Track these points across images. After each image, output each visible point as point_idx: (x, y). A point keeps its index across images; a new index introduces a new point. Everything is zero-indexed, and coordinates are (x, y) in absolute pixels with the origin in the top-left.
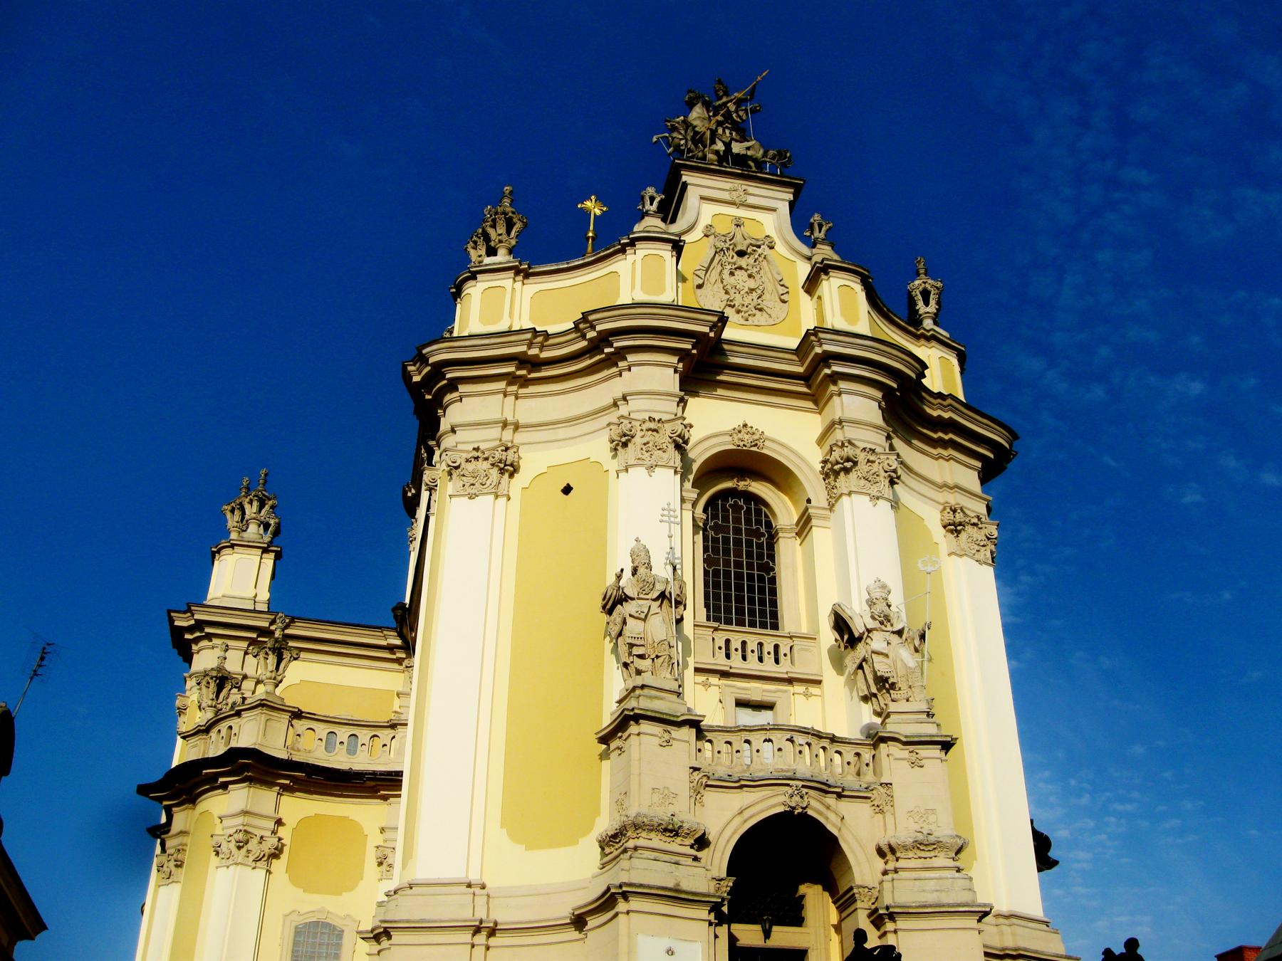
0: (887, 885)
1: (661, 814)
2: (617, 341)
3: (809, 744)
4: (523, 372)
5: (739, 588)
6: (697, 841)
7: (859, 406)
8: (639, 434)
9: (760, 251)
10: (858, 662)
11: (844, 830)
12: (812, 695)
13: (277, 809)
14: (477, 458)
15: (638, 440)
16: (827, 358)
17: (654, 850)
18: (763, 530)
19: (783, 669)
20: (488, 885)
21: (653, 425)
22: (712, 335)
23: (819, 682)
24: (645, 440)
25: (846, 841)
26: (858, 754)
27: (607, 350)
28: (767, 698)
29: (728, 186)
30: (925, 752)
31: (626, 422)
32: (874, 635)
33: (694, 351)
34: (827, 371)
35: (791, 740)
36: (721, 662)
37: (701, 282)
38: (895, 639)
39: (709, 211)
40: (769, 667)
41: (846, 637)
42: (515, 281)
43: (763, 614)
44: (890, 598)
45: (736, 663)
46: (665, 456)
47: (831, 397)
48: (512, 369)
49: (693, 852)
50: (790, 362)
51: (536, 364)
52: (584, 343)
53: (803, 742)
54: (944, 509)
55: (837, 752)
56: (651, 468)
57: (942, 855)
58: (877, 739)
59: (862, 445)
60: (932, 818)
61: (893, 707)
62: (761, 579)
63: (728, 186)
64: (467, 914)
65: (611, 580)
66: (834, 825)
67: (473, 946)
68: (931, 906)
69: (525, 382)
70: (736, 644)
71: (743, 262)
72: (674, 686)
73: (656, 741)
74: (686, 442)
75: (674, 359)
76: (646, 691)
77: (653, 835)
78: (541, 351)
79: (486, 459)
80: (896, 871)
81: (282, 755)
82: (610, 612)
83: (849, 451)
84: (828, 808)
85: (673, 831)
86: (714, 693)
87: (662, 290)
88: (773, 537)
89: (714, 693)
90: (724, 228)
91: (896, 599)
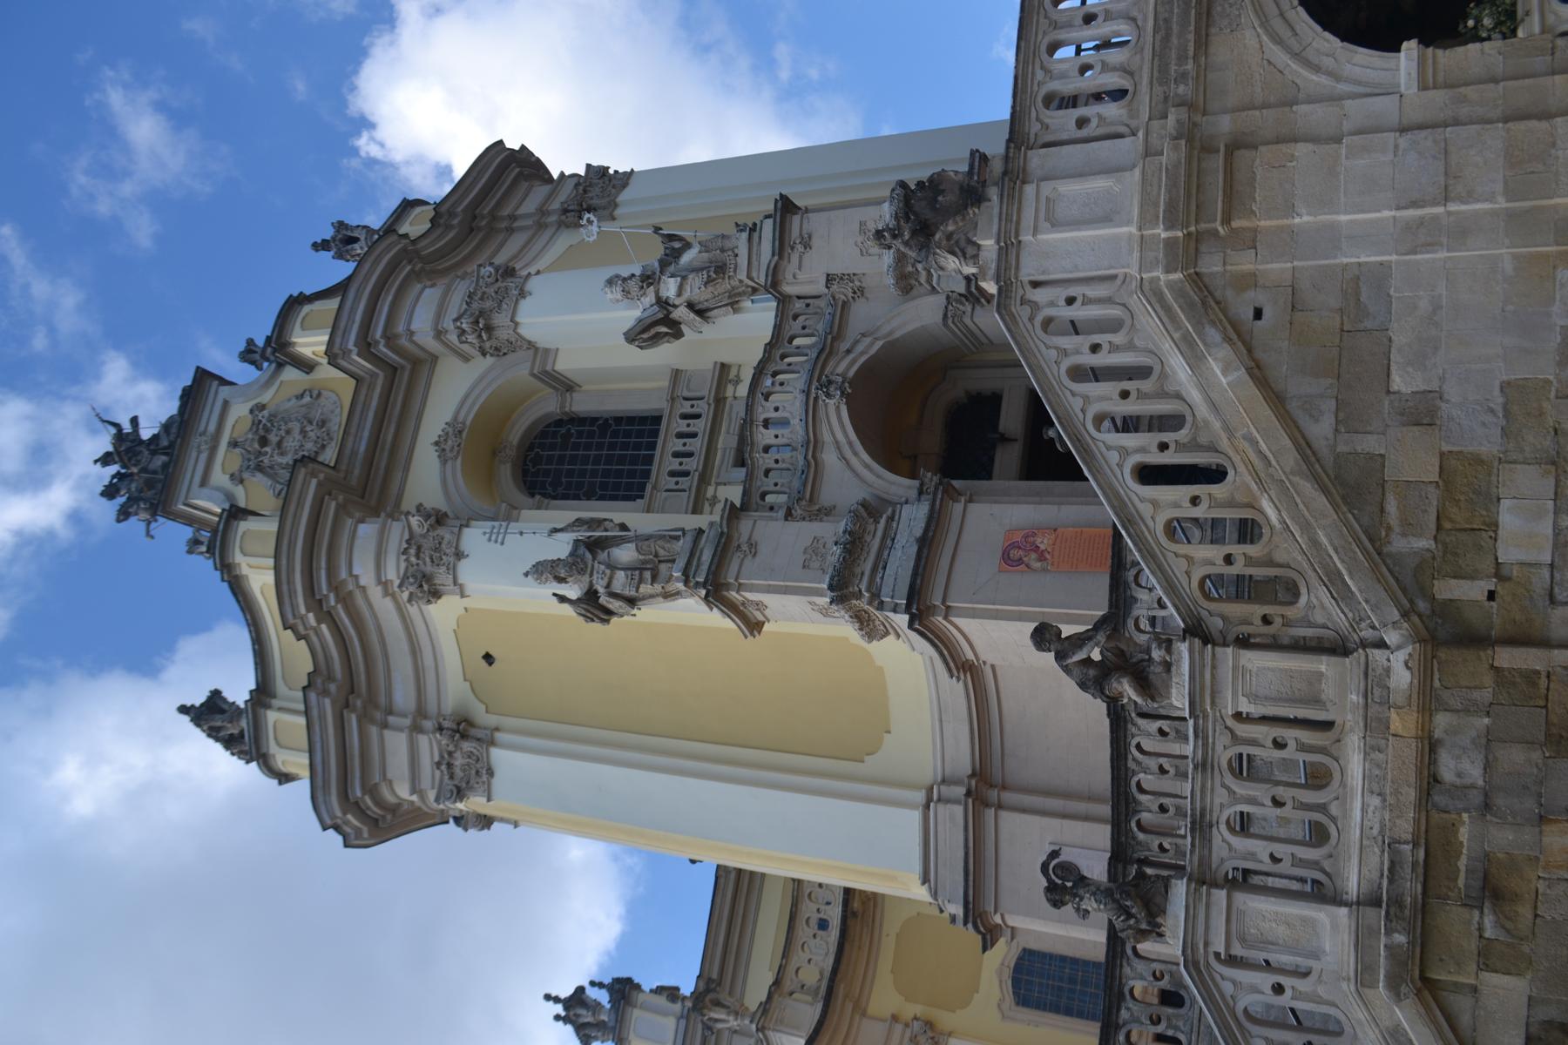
2: (320, 589)
3: (775, 374)
4: (359, 703)
6: (870, 514)
7: (425, 314)
8: (422, 567)
14: (449, 765)
15: (429, 568)
18: (563, 430)
21: (412, 551)
22: (322, 476)
23: (724, 368)
26: (795, 317)
27: (333, 603)
30: (795, 232)
35: (767, 397)
38: (672, 268)
39: (219, 477)
41: (664, 329)
42: (269, 707)
46: (448, 537)
48: (353, 720)
49: (883, 521)
50: (371, 387)
52: (324, 627)
53: (768, 382)
55: (791, 340)
56: (459, 555)
61: (742, 275)
63: (194, 454)
64: (958, 810)
65: (567, 609)
66: (872, 344)
67: (1000, 806)
69: (371, 701)
71: (273, 438)
73: (748, 562)
74: (437, 512)
77: (858, 570)
79: (450, 754)
81: (820, 1006)
82: (610, 613)
84: (848, 352)
85: (853, 545)
90: (236, 460)
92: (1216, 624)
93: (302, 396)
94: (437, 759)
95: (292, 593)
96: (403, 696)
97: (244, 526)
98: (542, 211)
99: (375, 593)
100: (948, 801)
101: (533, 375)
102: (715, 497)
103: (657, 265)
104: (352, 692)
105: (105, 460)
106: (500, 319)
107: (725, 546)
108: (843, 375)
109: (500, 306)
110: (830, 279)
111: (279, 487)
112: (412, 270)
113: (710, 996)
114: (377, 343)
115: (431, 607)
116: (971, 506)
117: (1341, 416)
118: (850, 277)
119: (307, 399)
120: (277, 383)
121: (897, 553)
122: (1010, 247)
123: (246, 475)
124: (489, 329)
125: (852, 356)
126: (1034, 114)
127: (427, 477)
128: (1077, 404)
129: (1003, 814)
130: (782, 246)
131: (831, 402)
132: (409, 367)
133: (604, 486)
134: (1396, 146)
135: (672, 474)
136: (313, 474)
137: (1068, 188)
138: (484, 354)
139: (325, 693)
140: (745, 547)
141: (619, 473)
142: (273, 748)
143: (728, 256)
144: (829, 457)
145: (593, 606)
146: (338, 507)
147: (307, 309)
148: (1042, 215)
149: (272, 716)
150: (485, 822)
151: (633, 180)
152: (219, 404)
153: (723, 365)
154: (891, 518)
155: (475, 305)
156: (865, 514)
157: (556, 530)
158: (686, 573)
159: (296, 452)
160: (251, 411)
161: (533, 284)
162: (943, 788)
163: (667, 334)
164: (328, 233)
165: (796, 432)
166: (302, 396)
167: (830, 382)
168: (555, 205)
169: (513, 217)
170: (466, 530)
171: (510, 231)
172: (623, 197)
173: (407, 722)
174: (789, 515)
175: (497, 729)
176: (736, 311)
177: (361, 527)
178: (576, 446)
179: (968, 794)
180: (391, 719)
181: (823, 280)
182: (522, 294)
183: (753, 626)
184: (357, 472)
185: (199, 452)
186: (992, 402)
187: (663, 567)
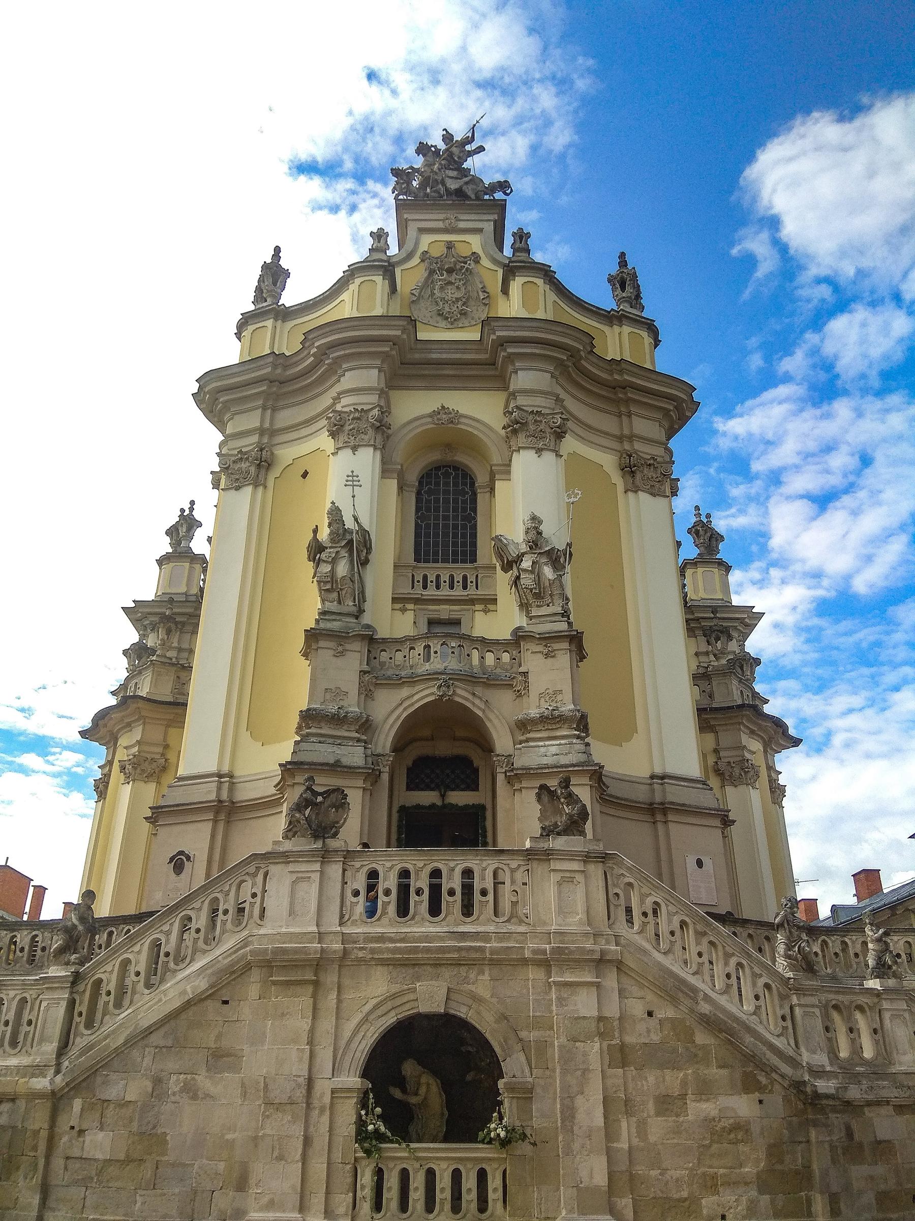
1: (332, 708)
5: (446, 535)
8: (348, 423)
9: (466, 266)
11: (487, 711)
12: (489, 611)
13: (165, 739)
15: (347, 428)
16: (503, 343)
19: (471, 591)
20: (237, 773)
21: (357, 415)
22: (405, 336)
23: (494, 601)
25: (490, 720)
28: (454, 616)
29: (442, 216)
30: (556, 646)
33: (394, 353)
34: (503, 354)
36: (419, 591)
39: (426, 240)
40: (458, 592)
42: (276, 320)
43: (464, 553)
45: (431, 592)
46: (366, 437)
49: (357, 735)
50: (478, 351)
53: (453, 644)
54: (621, 456)
55: (488, 651)
56: (354, 449)
57: (566, 725)
58: (519, 637)
60: (559, 697)
62: (464, 527)
63: (442, 216)
64: (213, 796)
66: (480, 709)
67: (215, 821)
70: (432, 577)
72: (354, 610)
73: (331, 652)
77: (323, 724)
80: (527, 741)
84: (474, 694)
85: (338, 719)
86: (410, 615)
88: (475, 494)
89: (410, 615)
92: (81, 988)
93: (484, 291)
95: (325, 335)
96: (286, 417)
97: (379, 279)
98: (631, 438)
99: (333, 393)
100: (219, 789)
102: (406, 610)
105: (448, 137)
106: (522, 439)
107: (340, 637)
108: (454, 693)
110: (525, 674)
113: (173, 626)
114: (505, 350)
115: (327, 433)
116: (360, 792)
117: (164, 1050)
118: (526, 688)
121: (331, 749)
122: (284, 857)
124: (515, 432)
125: (470, 697)
126: (365, 863)
127: (415, 406)
128: (197, 905)
129: (210, 824)
130: (547, 639)
131: (435, 690)
133: (428, 526)
134: (299, 1076)
135: (425, 577)
137: (314, 889)
138: (504, 428)
139: (275, 366)
141: (436, 535)
142: (251, 328)
143: (548, 599)
144: (405, 692)
147: (540, 282)
148: (300, 875)
149: (269, 323)
150: (216, 485)
151: (661, 502)
154: (359, 740)
155: (531, 417)
157: (356, 520)
159: (443, 299)
161: (549, 456)
163: (503, 562)
168: (638, 446)
170: (372, 449)
171: (620, 416)
173: (267, 425)
174: (363, 672)
177: (376, 371)
178: (456, 501)
179: (220, 801)
180: (269, 411)
181: (522, 670)
182: (539, 451)
184: (417, 356)
185: (443, 220)
186: (473, 786)
187: (335, 595)
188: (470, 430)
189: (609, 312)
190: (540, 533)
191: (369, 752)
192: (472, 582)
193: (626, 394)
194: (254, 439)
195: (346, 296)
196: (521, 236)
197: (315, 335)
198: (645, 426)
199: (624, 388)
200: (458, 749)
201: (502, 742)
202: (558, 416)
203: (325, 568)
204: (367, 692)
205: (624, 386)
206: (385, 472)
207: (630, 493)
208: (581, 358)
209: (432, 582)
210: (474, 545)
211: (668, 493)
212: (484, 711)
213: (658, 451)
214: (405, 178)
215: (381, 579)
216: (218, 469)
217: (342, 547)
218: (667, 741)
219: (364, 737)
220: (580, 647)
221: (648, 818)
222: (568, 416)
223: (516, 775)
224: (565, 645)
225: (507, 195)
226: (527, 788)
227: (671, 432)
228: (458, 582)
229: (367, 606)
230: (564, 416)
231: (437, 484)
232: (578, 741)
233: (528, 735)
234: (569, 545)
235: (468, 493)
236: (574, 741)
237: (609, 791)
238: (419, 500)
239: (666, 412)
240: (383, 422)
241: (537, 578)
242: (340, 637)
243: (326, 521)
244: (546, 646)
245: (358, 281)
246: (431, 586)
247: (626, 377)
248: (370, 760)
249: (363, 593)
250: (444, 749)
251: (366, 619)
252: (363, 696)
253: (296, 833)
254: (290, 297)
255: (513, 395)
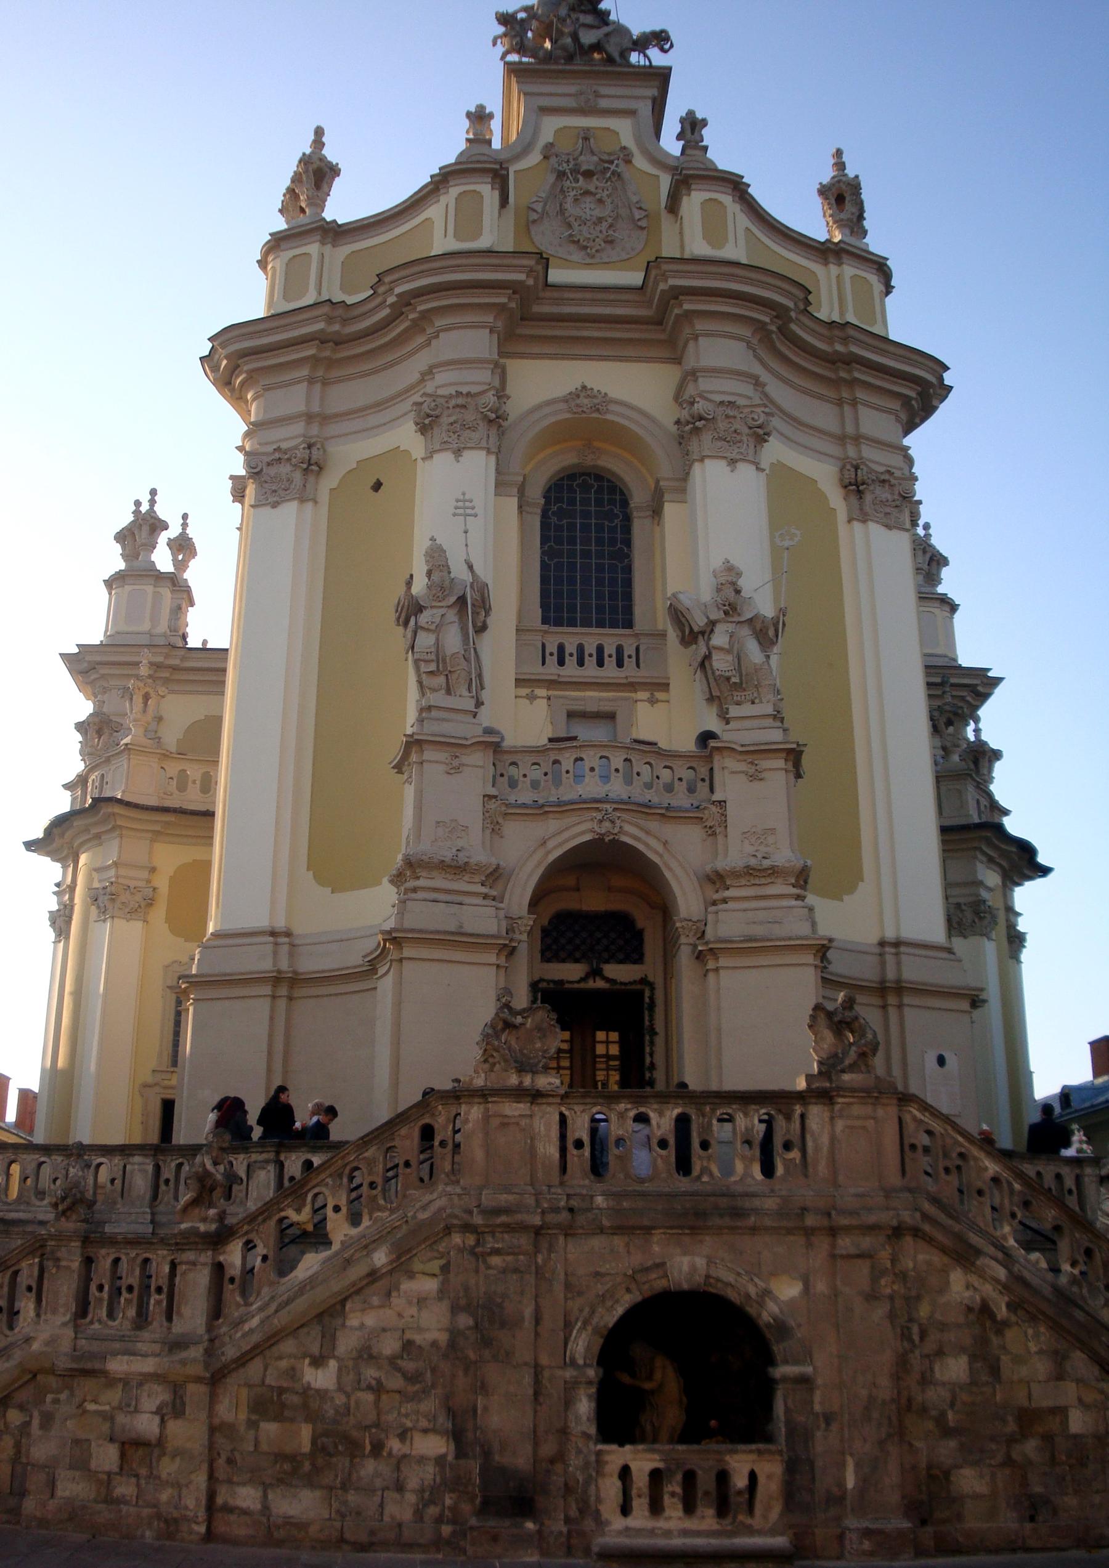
0: (710, 918)
8: (446, 413)
9: (613, 167)
10: (699, 659)
11: (666, 856)
12: (658, 701)
15: (445, 420)
16: (678, 293)
17: (435, 890)
21: (460, 401)
22: (531, 282)
23: (665, 687)
24: (452, 419)
25: (670, 869)
27: (411, 316)
28: (606, 707)
29: (573, 89)
31: (429, 400)
32: (719, 629)
37: (535, 216)
38: (745, 631)
39: (550, 126)
41: (687, 633)
44: (741, 582)
47: (687, 341)
49: (484, 890)
51: (339, 342)
52: (387, 311)
55: (665, 767)
56: (458, 453)
57: (780, 880)
59: (718, 398)
60: (771, 839)
63: (573, 89)
64: (266, 965)
68: (756, 940)
69: (331, 363)
73: (442, 768)
75: (490, 318)
76: (434, 713)
77: (435, 873)
78: (344, 326)
80: (725, 901)
82: (406, 624)
83: (700, 406)
85: (457, 868)
87: (477, 234)
88: (627, 519)
91: (747, 584)
93: (640, 208)
94: (284, 445)
98: (858, 439)
99: (422, 361)
100: (275, 953)
101: (657, 481)
103: (749, 616)
104: (337, 344)
109: (720, 439)
110: (722, 803)
111: (539, 207)
112: (764, 324)
114: (681, 306)
119: (638, 214)
120: (654, 171)
123: (553, 160)
124: (696, 431)
125: (642, 835)
129: (266, 1004)
132: (663, 337)
136: (530, 271)
139: (330, 320)
140: (456, 763)
141: (572, 581)
145: (410, 611)
146: (502, 307)
147: (727, 200)
150: (238, 494)
152: (632, 105)
153: (668, 684)
154: (485, 897)
156: (488, 872)
157: (470, 567)
158: (429, 708)
160: (625, 148)
161: (746, 470)
162: (286, 948)
163: (683, 632)
164: (850, 172)
165: (569, 791)
166: (640, 208)
167: (613, 822)
169: (854, 403)
170: (485, 452)
171: (840, 403)
172: (875, 529)
175: (316, 502)
176: (707, 700)
177: (488, 330)
178: (600, 528)
179: (279, 972)
181: (717, 797)
182: (732, 462)
183: (399, 768)
184: (546, 309)
186: (635, 955)
187: (441, 680)
188: (626, 423)
189: (823, 243)
190: (738, 592)
191: (502, 914)
192: (630, 657)
193: (850, 372)
194: (299, 428)
195: (434, 212)
196: (692, 126)
197: (396, 276)
198: (875, 422)
199: (848, 364)
200: (616, 904)
201: (688, 900)
202: (759, 410)
203: (425, 640)
204: (494, 828)
205: (851, 360)
206: (501, 486)
207: (856, 524)
208: (791, 320)
209: (571, 655)
210: (628, 596)
211: (908, 525)
212: (661, 856)
213: (895, 460)
214: (517, 27)
215: (500, 650)
216: (243, 472)
217: (448, 607)
218: (903, 889)
219: (494, 893)
220: (797, 764)
221: (877, 1001)
222: (774, 410)
223: (711, 949)
224: (780, 763)
225: (665, 51)
226: (727, 968)
227: (910, 427)
228: (610, 656)
229: (485, 695)
230: (767, 410)
231: (572, 502)
232: (799, 903)
233: (727, 894)
234: (783, 612)
235: (617, 516)
236: (794, 903)
237: (832, 968)
238: (545, 526)
239: (906, 401)
240: (500, 413)
241: (736, 660)
242: (454, 746)
243: (425, 568)
244: (752, 763)
245: (454, 191)
246: (571, 661)
247: (854, 349)
248: (504, 924)
249: (480, 676)
250: (594, 901)
251: (486, 717)
252: (488, 832)
253: (494, 1064)
254: (342, 206)
255: (692, 375)
